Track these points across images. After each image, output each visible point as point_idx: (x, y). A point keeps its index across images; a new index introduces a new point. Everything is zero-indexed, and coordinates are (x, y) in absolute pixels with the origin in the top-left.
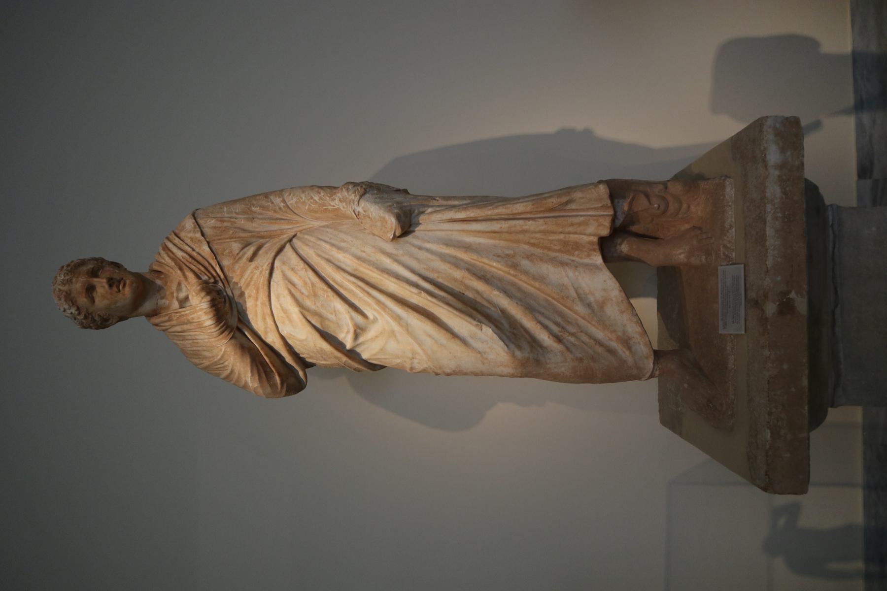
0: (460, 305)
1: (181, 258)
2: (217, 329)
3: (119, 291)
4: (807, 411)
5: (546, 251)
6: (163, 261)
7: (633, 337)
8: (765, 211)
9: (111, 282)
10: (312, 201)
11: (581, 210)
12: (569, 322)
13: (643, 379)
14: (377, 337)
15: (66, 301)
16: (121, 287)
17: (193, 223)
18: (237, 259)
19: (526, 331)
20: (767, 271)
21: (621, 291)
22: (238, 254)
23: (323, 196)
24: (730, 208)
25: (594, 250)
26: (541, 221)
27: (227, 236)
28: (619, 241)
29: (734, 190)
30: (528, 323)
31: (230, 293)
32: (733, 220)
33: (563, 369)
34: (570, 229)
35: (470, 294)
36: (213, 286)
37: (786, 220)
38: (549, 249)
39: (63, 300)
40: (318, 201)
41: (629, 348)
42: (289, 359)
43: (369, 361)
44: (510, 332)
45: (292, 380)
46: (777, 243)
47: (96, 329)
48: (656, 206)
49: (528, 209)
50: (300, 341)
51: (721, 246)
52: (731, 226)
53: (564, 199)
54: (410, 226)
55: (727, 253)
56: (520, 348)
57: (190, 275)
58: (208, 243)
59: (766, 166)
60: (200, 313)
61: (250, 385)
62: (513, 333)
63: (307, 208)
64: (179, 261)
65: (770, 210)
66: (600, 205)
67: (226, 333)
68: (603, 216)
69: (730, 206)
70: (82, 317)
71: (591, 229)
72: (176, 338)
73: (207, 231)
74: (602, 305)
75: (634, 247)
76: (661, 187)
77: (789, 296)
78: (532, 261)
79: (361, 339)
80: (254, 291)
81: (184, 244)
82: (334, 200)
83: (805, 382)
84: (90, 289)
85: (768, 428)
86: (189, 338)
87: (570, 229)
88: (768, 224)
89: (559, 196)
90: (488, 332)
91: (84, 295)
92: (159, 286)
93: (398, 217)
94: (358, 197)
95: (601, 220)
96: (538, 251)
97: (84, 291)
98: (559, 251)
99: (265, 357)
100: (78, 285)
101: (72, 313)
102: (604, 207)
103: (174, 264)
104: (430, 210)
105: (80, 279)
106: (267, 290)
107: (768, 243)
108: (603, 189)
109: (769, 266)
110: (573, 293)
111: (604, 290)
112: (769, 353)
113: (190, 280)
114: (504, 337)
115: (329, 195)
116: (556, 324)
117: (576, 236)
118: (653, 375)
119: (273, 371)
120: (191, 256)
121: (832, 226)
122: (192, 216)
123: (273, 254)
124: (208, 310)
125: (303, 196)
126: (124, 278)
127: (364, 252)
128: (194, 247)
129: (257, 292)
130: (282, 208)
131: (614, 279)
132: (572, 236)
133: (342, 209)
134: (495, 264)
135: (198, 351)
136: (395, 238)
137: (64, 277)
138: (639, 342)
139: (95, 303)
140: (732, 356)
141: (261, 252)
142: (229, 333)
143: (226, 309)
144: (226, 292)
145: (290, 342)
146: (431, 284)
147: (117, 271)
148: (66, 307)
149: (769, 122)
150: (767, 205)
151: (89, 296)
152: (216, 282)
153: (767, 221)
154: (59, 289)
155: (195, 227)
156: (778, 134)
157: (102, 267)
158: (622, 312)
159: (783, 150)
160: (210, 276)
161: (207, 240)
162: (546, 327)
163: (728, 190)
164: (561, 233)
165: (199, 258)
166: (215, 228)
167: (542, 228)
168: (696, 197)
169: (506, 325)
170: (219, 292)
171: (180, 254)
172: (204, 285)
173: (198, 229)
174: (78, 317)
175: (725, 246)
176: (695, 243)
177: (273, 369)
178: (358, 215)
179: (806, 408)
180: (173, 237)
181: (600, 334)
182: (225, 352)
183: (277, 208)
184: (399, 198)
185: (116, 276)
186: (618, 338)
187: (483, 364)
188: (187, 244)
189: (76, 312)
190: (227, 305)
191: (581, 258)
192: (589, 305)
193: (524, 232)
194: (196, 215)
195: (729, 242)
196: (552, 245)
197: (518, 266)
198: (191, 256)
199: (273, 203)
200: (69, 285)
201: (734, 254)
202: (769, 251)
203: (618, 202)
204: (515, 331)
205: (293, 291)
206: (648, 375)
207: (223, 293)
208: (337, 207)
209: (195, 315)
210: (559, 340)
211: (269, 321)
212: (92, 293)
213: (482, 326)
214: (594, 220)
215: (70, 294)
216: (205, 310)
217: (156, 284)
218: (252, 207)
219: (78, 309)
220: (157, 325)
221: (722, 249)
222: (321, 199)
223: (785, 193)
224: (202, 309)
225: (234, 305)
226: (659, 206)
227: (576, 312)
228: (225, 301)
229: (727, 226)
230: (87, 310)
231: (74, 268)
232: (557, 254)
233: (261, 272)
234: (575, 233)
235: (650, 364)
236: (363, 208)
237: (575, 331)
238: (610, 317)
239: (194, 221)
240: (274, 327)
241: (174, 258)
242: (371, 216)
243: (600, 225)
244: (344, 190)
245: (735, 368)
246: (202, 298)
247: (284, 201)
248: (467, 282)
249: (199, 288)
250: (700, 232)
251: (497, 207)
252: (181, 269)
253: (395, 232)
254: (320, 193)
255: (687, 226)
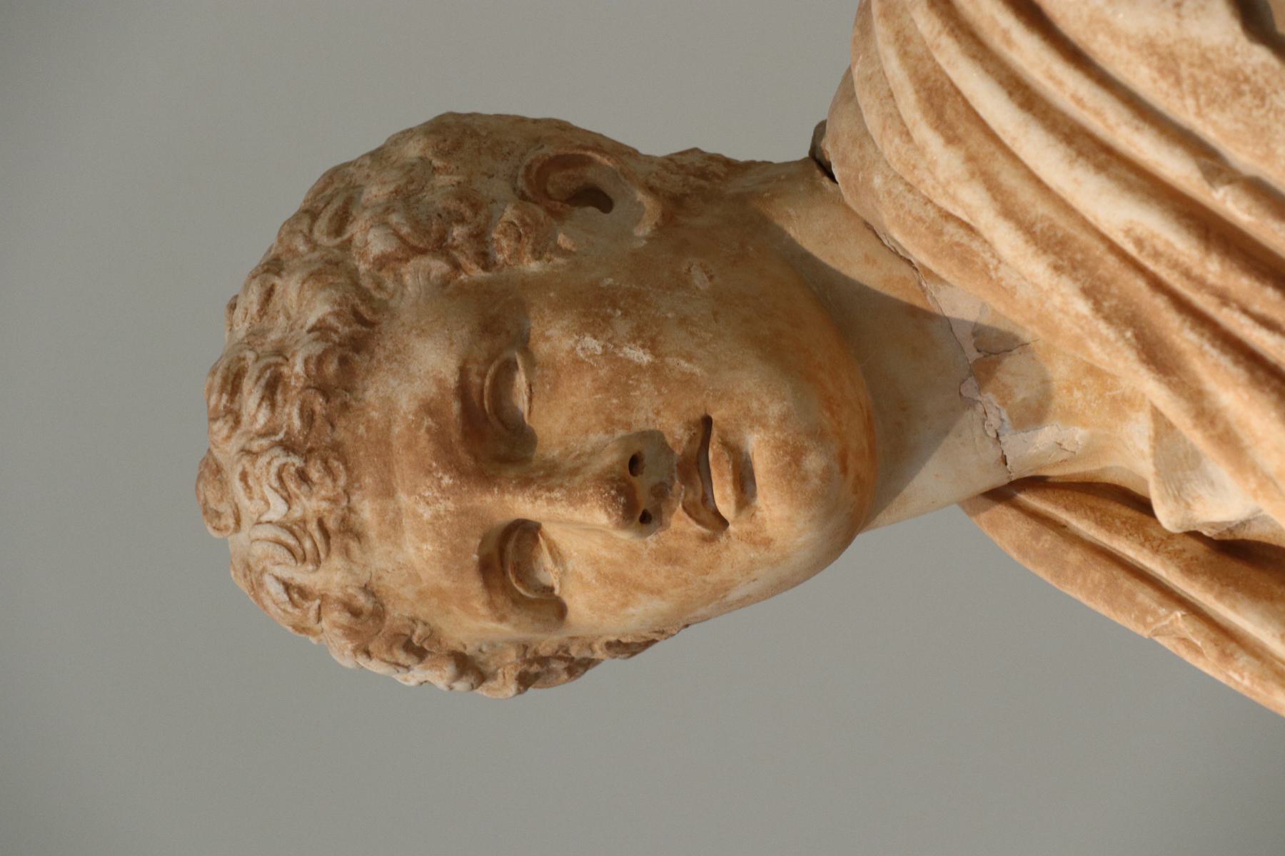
16: (724, 498)
64: (1111, 260)
91: (479, 604)
92: (978, 332)
97: (474, 585)
103: (1082, 307)
105: (403, 498)
137: (288, 500)
139: (571, 616)
147: (640, 356)
151: (518, 601)
154: (287, 587)
200: (346, 552)
212: (525, 571)
215: (379, 614)
217: (947, 323)
231: (319, 404)
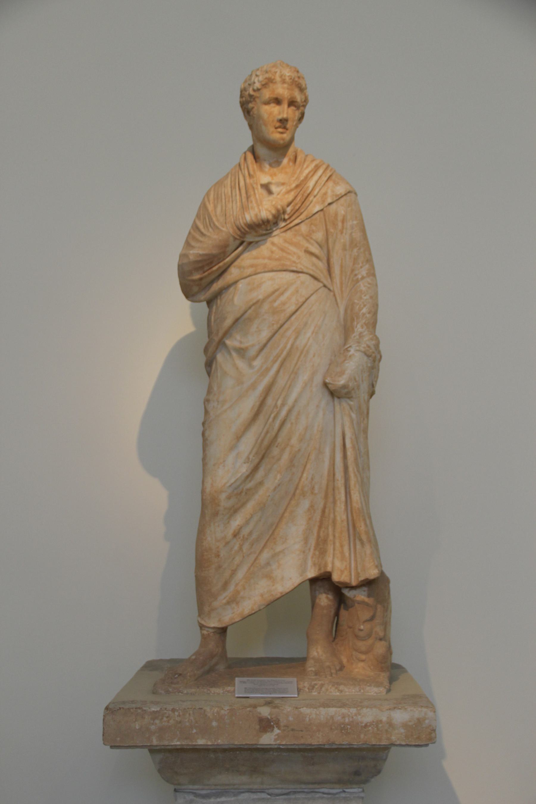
0: (266, 443)
1: (307, 185)
2: (243, 225)
3: (276, 128)
4: (175, 743)
5: (318, 524)
6: (305, 166)
7: (238, 607)
8: (350, 708)
9: (283, 122)
10: (362, 306)
11: (355, 556)
12: (252, 545)
13: (199, 619)
14: (237, 368)
15: (266, 78)
16: (280, 130)
17: (341, 194)
18: (308, 237)
19: (244, 504)
20: (297, 708)
21: (281, 593)
22: (311, 238)
23: (366, 317)
24: (358, 690)
25: (320, 569)
26: (344, 517)
27: (328, 227)
28: (330, 596)
29: (375, 694)
30: (250, 506)
31: (275, 233)
32: (347, 693)
33: (209, 539)
34: (338, 544)
35: (275, 451)
36: (281, 218)
37: (342, 726)
38: (320, 527)
39: (267, 75)
40: (362, 312)
41: (228, 603)
42: (216, 287)
43: (214, 363)
44: (243, 489)
45: (195, 289)
46: (322, 717)
47: (240, 102)
48: (362, 627)
49: (354, 505)
50: (232, 299)
51: (322, 682)
52: (341, 691)
53: (364, 537)
54: (339, 398)
55: (316, 687)
56: (229, 498)
57: (290, 197)
58: (322, 210)
59: (390, 709)
60: (256, 210)
61: (191, 252)
62: (241, 492)
63: (356, 301)
65: (351, 711)
66: (359, 571)
67: (239, 233)
68: (351, 575)
69: (360, 691)
70: (252, 93)
71: (338, 564)
72: (233, 179)
73: (334, 206)
74: (269, 576)
75: (325, 611)
76: (381, 634)
77: (275, 727)
78: (309, 510)
79: (234, 354)
80: (277, 257)
81: (320, 187)
82: (362, 327)
83: (201, 742)
84: (278, 101)
85: (161, 709)
86: (234, 194)
87: (338, 544)
88: (339, 709)
89: (367, 533)
90: (244, 469)
91: (272, 96)
93: (344, 387)
94: (363, 350)
95: (346, 573)
96: (317, 516)
97: (275, 96)
98: (318, 536)
99: (216, 267)
100: (282, 90)
101: (254, 83)
102: (358, 574)
104: (354, 416)
106: (278, 269)
107: (321, 709)
108: (372, 573)
109: (302, 710)
110: (279, 548)
111: (282, 578)
112: (226, 709)
113: (286, 196)
114: (238, 483)
115: (367, 322)
116: (250, 533)
117: (332, 551)
118: (203, 628)
119: (204, 272)
120: (309, 195)
121: (344, 792)
122: (348, 191)
123: (311, 273)
124: (259, 217)
125: (367, 297)
126: (288, 132)
127: (314, 356)
128: (317, 197)
129: (277, 260)
130: (357, 277)
131: (292, 587)
132: (332, 547)
133: (354, 335)
134: (305, 475)
135: (221, 201)
136: (325, 385)
137: (289, 76)
138: (234, 613)
140: (222, 692)
141: (314, 259)
142: (238, 235)
143: (261, 231)
144: (276, 230)
145: (232, 289)
146: (285, 417)
148: (261, 78)
149: (430, 714)
150: (355, 709)
151: (270, 100)
152: (285, 220)
153: (341, 709)
155: (336, 195)
156: (420, 721)
157: (298, 108)
158: (262, 595)
159: (405, 725)
160: (290, 215)
161: (325, 209)
162: (247, 522)
163: (376, 689)
164: (334, 536)
165: (307, 203)
166: (336, 215)
167: (338, 518)
168: (372, 667)
169: (250, 485)
170: (276, 223)
171: (311, 184)
172: (282, 212)
173: (335, 199)
174: (251, 89)
175: (322, 685)
176: (328, 664)
177: (206, 273)
178: (347, 350)
179: (178, 743)
180: (328, 174)
181: (240, 575)
182: (221, 231)
183: (356, 272)
184: (365, 387)
185: (289, 125)
186: (237, 592)
187: (214, 465)
188: (320, 190)
189: (255, 88)
190: (264, 232)
191: (312, 557)
192: (268, 564)
193: (335, 502)
194: (349, 194)
195: (327, 690)
196: (323, 529)
197: (304, 496)
198: (309, 195)
199: (361, 267)
201: (316, 693)
202: (315, 710)
203: (364, 591)
204: (243, 494)
205: (277, 293)
206: (203, 622)
207: (275, 227)
208: (356, 330)
209: (255, 205)
210: (235, 535)
211: (249, 271)
212: (274, 102)
213: (248, 462)
214: (346, 566)
216: (259, 214)
218: (358, 248)
219: (258, 90)
220: (245, 159)
221: (320, 682)
222: (364, 314)
223: (366, 726)
224: (260, 212)
225: (264, 238)
226: (362, 630)
227: (261, 551)
228: (267, 230)
229: (341, 687)
230: (258, 97)
232: (315, 534)
233: (294, 262)
234: (334, 550)
235: (214, 623)
236: (353, 355)
237: (244, 551)
238: (257, 584)
239: (343, 194)
240: (245, 275)
241: (306, 179)
242: (347, 361)
243: (342, 572)
244: (371, 336)
245: (211, 694)
246: (270, 211)
247: (363, 278)
248: (288, 450)
249: (279, 207)
250: (338, 668)
251: (355, 475)
252: (297, 186)
253: (331, 384)
254: (369, 313)
255: (345, 660)
